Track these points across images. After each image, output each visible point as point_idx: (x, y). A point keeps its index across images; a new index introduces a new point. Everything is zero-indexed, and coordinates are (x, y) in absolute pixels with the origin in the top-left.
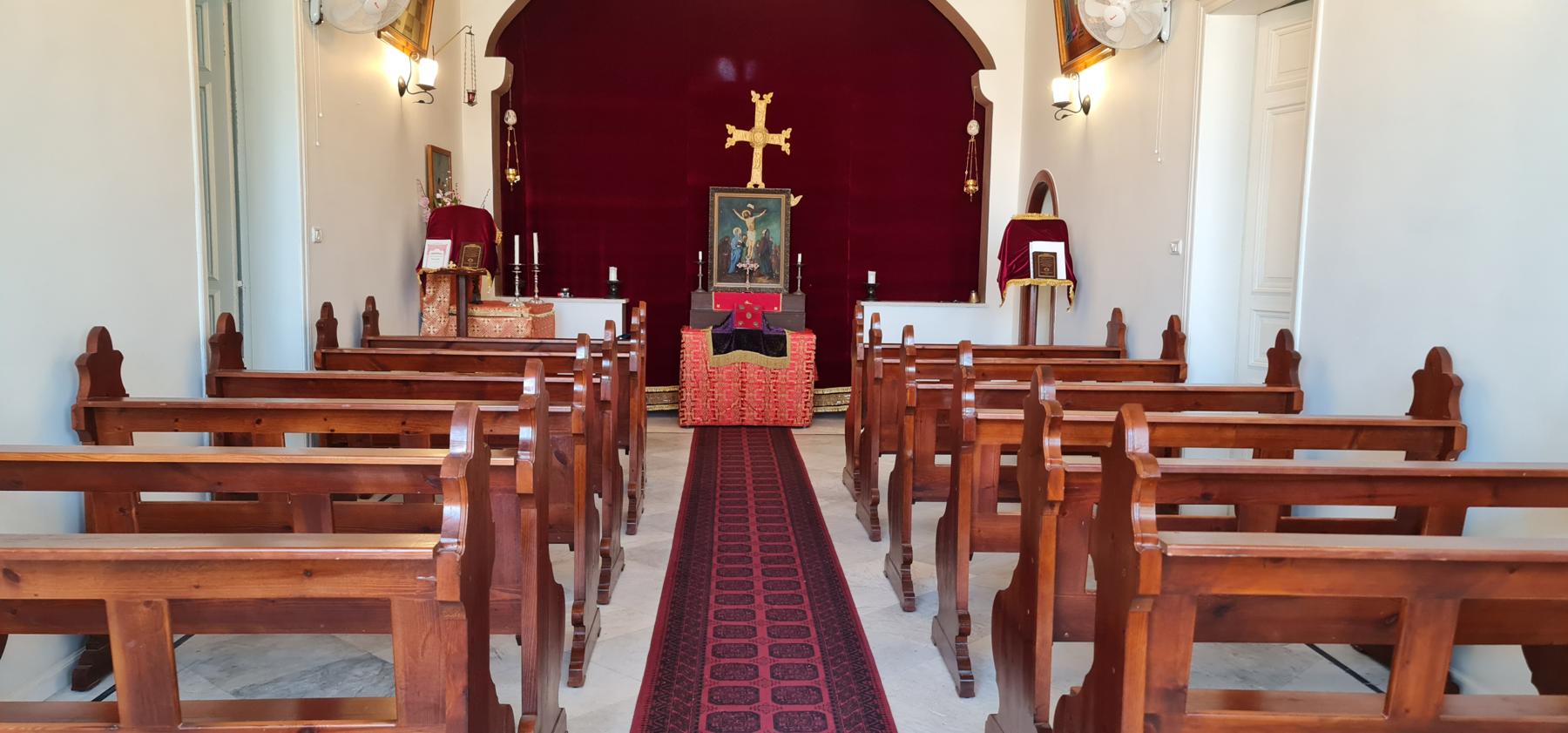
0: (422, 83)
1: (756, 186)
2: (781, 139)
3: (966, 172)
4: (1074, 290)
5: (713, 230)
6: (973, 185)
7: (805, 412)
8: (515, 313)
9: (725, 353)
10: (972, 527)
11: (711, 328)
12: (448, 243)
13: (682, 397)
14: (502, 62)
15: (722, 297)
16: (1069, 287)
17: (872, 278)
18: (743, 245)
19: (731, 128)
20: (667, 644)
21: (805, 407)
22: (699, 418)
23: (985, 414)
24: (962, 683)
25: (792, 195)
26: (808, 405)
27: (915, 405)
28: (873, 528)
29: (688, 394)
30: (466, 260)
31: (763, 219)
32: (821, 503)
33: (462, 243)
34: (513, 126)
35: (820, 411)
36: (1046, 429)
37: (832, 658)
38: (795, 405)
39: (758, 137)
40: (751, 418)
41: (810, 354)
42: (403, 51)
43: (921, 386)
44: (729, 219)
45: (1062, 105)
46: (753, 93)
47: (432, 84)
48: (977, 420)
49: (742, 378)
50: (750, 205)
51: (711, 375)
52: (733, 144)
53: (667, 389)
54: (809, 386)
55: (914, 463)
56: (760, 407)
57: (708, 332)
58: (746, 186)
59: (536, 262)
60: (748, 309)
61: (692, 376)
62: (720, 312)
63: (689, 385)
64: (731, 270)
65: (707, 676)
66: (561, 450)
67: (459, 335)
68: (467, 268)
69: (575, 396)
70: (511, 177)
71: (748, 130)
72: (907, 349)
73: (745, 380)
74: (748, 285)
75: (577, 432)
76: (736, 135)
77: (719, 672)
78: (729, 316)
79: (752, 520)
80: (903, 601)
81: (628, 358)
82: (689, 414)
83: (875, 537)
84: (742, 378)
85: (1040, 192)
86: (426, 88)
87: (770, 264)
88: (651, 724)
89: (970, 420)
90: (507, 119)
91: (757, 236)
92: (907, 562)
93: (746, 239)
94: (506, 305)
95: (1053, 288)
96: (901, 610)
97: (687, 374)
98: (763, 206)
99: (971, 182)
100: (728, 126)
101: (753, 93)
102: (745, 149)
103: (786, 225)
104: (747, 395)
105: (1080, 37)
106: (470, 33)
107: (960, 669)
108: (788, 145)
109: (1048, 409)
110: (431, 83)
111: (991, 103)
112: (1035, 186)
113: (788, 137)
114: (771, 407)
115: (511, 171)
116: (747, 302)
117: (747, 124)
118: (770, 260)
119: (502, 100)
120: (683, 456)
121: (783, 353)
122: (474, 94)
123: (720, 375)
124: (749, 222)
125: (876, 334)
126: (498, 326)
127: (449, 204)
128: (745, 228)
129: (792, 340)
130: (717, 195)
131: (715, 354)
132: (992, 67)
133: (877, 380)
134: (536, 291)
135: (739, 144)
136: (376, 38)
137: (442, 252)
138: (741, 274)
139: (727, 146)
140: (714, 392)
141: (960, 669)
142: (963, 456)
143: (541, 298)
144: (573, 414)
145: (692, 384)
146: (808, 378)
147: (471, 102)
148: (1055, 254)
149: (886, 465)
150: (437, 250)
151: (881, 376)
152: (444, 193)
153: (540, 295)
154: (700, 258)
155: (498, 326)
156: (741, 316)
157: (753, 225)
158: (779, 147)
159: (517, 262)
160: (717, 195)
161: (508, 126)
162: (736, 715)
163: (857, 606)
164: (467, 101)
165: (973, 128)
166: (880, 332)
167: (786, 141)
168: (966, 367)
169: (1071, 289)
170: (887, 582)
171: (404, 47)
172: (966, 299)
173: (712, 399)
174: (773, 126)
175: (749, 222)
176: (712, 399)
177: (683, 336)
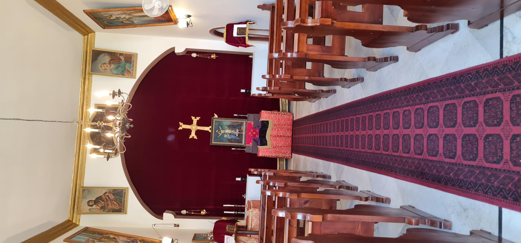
1: (210, 129)
2: (195, 120)
3: (209, 58)
4: (250, 22)
5: (225, 144)
6: (213, 56)
7: (288, 115)
8: (251, 214)
9: (267, 142)
10: (336, 55)
11: (258, 146)
12: (226, 236)
13: (281, 157)
14: (165, 215)
15: (248, 142)
16: (249, 23)
17: (243, 91)
18: (230, 134)
19: (191, 137)
20: (374, 167)
21: (286, 115)
22: (289, 152)
23: (296, 49)
24: (393, 60)
25: (214, 117)
26: (286, 114)
27: (290, 75)
28: (331, 92)
29: (280, 155)
30: (232, 230)
31: (222, 127)
32: (321, 110)
33: (226, 231)
34: (187, 211)
35: (288, 110)
36: (305, 25)
37: (381, 107)
38: (286, 118)
39: (194, 128)
40: (289, 134)
41: (268, 113)
43: (283, 73)
44: (221, 139)
45: (188, 24)
46: (179, 129)
47: (171, 239)
48: (298, 52)
49: (275, 136)
50: (217, 131)
51: (274, 147)
52: (196, 136)
53: (278, 162)
54: (279, 113)
55: (310, 76)
56: (286, 130)
57: (260, 147)
58: (210, 132)
59: (233, 206)
60: (252, 133)
61: (274, 153)
62: (253, 143)
63: (277, 155)
64: (238, 138)
65: (387, 153)
66: (303, 202)
67: (258, 234)
68: (235, 230)
69: (284, 196)
70: (204, 213)
71: (191, 131)
72: (270, 77)
73: (276, 135)
74: (244, 133)
75: (297, 196)
76: (193, 135)
77: (386, 148)
78: (254, 140)
79: (327, 134)
80: (360, 81)
81: (269, 176)
82: (287, 155)
83: (335, 91)
84: (275, 136)
85: (216, 33)
87: (237, 125)
88: (406, 174)
89: (298, 55)
90: (184, 213)
91: (227, 129)
92: (346, 80)
93: (228, 133)
94: (248, 217)
95: (249, 29)
96: (363, 83)
97: (273, 155)
98: (217, 127)
99: (212, 56)
100: (190, 138)
101: (179, 129)
102: (198, 132)
103: (224, 119)
104: (281, 135)
105: (165, 18)
106: (155, 225)
107: (388, 61)
108: (197, 117)
109: (297, 24)
111: (186, 49)
113: (194, 117)
114: (286, 127)
115: (202, 213)
116: (250, 134)
117: (189, 131)
118: (236, 125)
119: (178, 215)
120: (302, 157)
121: (268, 122)
122: (175, 225)
123: (274, 144)
124: (222, 132)
125: (264, 89)
126: (255, 220)
127: (212, 235)
128: (224, 133)
129: (263, 118)
130: (213, 143)
131: (267, 145)
132: (174, 48)
133: (279, 89)
134: (243, 206)
135: (196, 134)
137: (229, 239)
138: (240, 135)
139: (196, 138)
140: (280, 146)
141: (388, 61)
142: (310, 58)
143: (246, 205)
144: (290, 197)
145: (277, 153)
146: (276, 114)
147: (178, 226)
148: (238, 28)
149: (309, 87)
150: (228, 240)
151: (278, 87)
152: (208, 237)
153: (244, 205)
154: (234, 149)
155: (255, 220)
156: (254, 136)
157: (224, 131)
158: (198, 121)
159: (233, 212)
160: (213, 143)
161: (187, 213)
162: (403, 143)
163: (361, 98)
164: (177, 227)
165: (194, 55)
166: (263, 88)
167: (196, 118)
168: (278, 55)
169: (250, 23)
170: (352, 88)
172: (252, 59)
173: (283, 147)
174: (190, 123)
175: (222, 132)
176: (283, 147)
177: (260, 156)
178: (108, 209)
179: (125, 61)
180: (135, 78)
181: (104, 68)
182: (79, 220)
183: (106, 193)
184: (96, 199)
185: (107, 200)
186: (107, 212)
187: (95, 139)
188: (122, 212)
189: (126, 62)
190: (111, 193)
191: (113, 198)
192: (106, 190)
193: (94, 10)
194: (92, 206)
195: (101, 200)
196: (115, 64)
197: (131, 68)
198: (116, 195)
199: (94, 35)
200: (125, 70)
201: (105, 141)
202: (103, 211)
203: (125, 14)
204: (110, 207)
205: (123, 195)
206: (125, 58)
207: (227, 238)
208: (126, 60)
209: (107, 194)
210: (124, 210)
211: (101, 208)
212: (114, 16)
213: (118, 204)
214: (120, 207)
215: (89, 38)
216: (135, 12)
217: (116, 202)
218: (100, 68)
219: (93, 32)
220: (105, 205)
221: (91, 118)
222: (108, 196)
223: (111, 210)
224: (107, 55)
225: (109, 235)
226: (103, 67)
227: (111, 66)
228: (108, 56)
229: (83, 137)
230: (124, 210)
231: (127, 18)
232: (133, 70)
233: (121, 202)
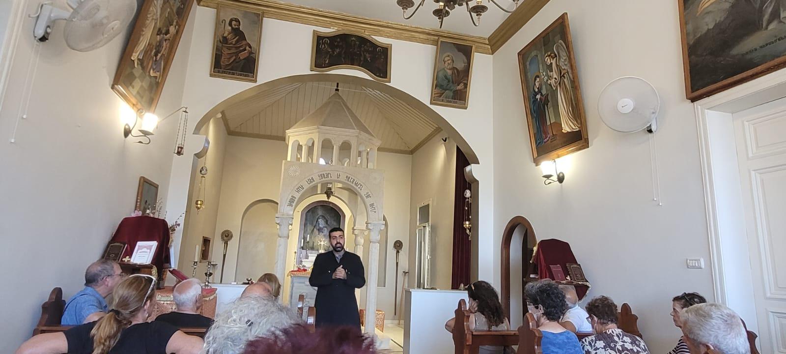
0: (143, 129)
45: (548, 177)
47: (151, 131)
86: (145, 133)
105: (551, 142)
106: (186, 112)
110: (151, 130)
111: (478, 181)
112: (509, 226)
122: (182, 148)
132: (477, 162)
136: (110, 89)
147: (179, 153)
164: (176, 152)
171: (134, 105)
178: (222, 49)
180: (431, 103)
181: (446, 59)
183: (250, 47)
184: (241, 31)
185: (237, 48)
186: (217, 46)
187: (339, 40)
188: (214, 69)
189: (454, 91)
190: (249, 55)
191: (241, 58)
192: (256, 48)
193: (569, 27)
194: (230, 24)
195: (237, 40)
196: (452, 77)
197: (446, 98)
199: (490, 54)
200: (443, 89)
201: (335, 53)
202: (219, 39)
203: (562, 76)
204: (226, 52)
205: (245, 73)
206: (460, 90)
208: (458, 93)
209: (247, 48)
210: (219, 72)
212: (554, 62)
214: (222, 66)
215: (484, 45)
216: (567, 91)
220: (231, 44)
221: (372, 37)
222: (245, 50)
224: (465, 66)
225: (175, 27)
226: (446, 59)
227: (450, 69)
229: (342, 23)
230: (219, 72)
231: (549, 82)
232: (443, 101)
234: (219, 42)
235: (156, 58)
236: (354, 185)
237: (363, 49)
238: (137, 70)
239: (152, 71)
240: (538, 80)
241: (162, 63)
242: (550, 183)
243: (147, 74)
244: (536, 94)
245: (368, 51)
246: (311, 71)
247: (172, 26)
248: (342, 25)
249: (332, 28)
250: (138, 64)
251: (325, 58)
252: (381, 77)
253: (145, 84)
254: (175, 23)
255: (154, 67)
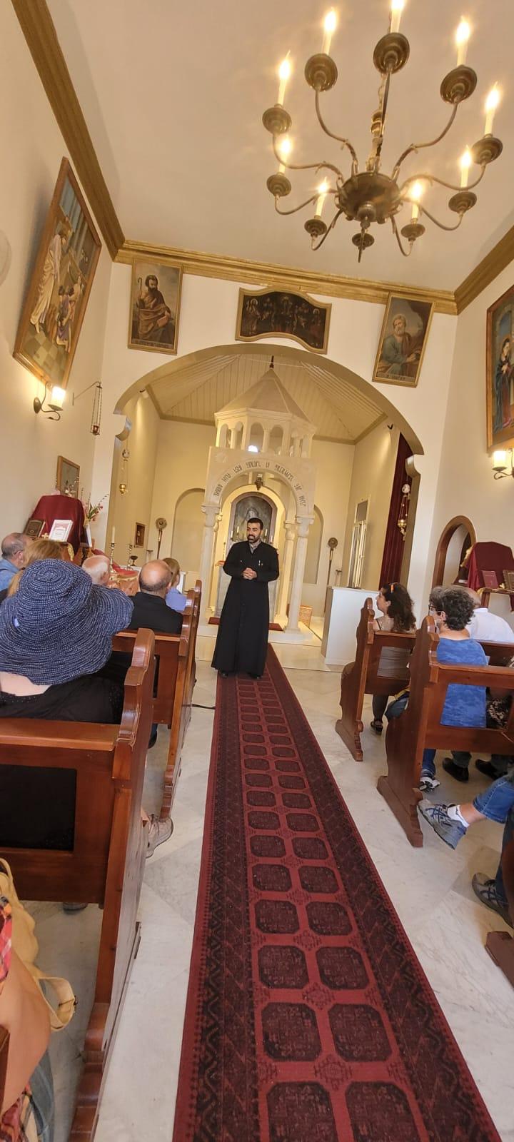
0: (52, 403)
42: (41, 380)
45: (499, 470)
47: (60, 406)
86: (55, 409)
106: (100, 387)
110: (60, 405)
111: (419, 475)
112: (450, 526)
122: (98, 427)
132: (421, 452)
136: (12, 357)
147: (95, 432)
179: (406, 363)
180: (373, 380)
181: (397, 322)
182: (123, 263)
183: (169, 311)
185: (156, 313)
187: (268, 300)
190: (169, 321)
194: (147, 284)
197: (392, 373)
198: (164, 331)
199: (454, 314)
204: (143, 318)
207: (65, 526)
209: (166, 313)
210: (137, 343)
211: (142, 301)
213: (146, 334)
215: (447, 303)
217: (152, 329)
218: (397, 316)
219: (458, 310)
220: (147, 308)
222: (163, 315)
223: (136, 320)
226: (397, 322)
227: (400, 335)
228: (417, 331)
232: (388, 377)
233: (151, 339)
234: (136, 307)
235: (61, 324)
236: (284, 476)
237: (296, 311)
238: (41, 337)
239: (58, 339)
240: (507, 345)
241: (70, 329)
242: (502, 477)
243: (53, 342)
244: (502, 364)
245: (301, 314)
246: (236, 340)
247: (76, 285)
248: (273, 280)
249: (261, 284)
250: (40, 329)
251: (253, 323)
252: (316, 347)
253: (53, 353)
254: (79, 281)
255: (61, 334)
